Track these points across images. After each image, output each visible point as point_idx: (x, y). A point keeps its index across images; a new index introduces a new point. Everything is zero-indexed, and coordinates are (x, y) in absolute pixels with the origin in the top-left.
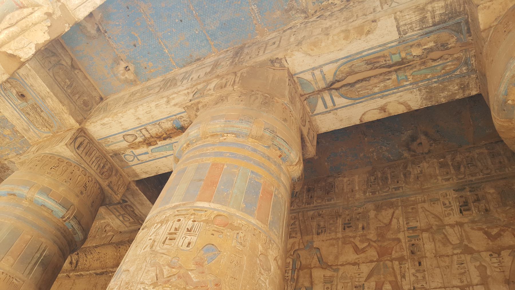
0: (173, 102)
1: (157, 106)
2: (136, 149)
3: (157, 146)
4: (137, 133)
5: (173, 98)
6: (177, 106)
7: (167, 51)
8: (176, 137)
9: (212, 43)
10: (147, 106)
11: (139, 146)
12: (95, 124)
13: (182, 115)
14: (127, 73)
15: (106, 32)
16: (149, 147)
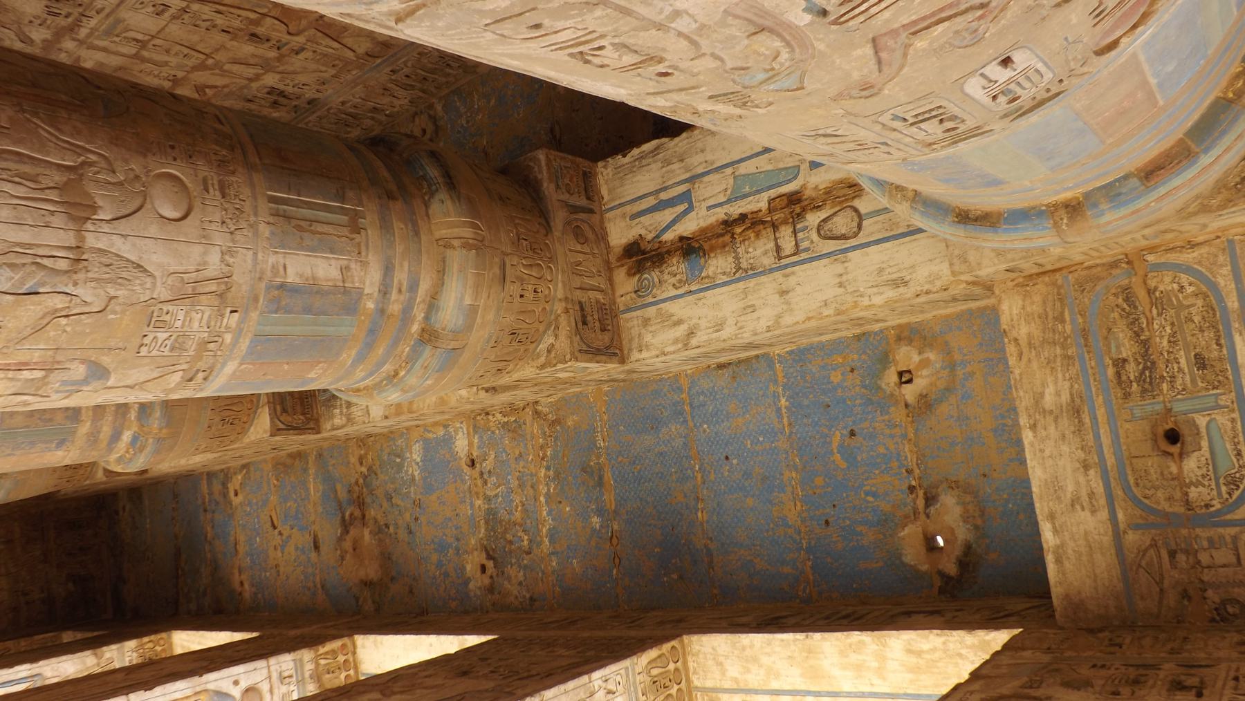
0: (681, 331)
1: (719, 326)
2: (841, 182)
3: (773, 193)
4: (812, 242)
5: (676, 341)
6: (675, 318)
7: (783, 400)
8: (711, 224)
9: (683, 396)
10: (742, 330)
11: (828, 192)
12: (926, 287)
13: (674, 292)
14: (911, 368)
15: (912, 489)
16: (798, 188)
